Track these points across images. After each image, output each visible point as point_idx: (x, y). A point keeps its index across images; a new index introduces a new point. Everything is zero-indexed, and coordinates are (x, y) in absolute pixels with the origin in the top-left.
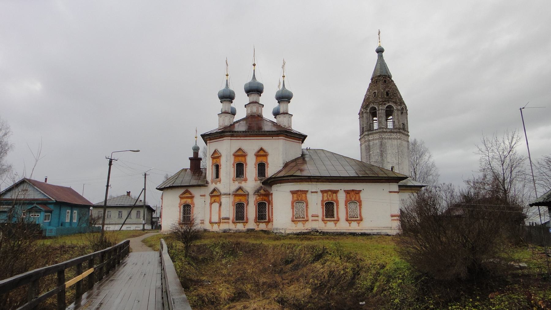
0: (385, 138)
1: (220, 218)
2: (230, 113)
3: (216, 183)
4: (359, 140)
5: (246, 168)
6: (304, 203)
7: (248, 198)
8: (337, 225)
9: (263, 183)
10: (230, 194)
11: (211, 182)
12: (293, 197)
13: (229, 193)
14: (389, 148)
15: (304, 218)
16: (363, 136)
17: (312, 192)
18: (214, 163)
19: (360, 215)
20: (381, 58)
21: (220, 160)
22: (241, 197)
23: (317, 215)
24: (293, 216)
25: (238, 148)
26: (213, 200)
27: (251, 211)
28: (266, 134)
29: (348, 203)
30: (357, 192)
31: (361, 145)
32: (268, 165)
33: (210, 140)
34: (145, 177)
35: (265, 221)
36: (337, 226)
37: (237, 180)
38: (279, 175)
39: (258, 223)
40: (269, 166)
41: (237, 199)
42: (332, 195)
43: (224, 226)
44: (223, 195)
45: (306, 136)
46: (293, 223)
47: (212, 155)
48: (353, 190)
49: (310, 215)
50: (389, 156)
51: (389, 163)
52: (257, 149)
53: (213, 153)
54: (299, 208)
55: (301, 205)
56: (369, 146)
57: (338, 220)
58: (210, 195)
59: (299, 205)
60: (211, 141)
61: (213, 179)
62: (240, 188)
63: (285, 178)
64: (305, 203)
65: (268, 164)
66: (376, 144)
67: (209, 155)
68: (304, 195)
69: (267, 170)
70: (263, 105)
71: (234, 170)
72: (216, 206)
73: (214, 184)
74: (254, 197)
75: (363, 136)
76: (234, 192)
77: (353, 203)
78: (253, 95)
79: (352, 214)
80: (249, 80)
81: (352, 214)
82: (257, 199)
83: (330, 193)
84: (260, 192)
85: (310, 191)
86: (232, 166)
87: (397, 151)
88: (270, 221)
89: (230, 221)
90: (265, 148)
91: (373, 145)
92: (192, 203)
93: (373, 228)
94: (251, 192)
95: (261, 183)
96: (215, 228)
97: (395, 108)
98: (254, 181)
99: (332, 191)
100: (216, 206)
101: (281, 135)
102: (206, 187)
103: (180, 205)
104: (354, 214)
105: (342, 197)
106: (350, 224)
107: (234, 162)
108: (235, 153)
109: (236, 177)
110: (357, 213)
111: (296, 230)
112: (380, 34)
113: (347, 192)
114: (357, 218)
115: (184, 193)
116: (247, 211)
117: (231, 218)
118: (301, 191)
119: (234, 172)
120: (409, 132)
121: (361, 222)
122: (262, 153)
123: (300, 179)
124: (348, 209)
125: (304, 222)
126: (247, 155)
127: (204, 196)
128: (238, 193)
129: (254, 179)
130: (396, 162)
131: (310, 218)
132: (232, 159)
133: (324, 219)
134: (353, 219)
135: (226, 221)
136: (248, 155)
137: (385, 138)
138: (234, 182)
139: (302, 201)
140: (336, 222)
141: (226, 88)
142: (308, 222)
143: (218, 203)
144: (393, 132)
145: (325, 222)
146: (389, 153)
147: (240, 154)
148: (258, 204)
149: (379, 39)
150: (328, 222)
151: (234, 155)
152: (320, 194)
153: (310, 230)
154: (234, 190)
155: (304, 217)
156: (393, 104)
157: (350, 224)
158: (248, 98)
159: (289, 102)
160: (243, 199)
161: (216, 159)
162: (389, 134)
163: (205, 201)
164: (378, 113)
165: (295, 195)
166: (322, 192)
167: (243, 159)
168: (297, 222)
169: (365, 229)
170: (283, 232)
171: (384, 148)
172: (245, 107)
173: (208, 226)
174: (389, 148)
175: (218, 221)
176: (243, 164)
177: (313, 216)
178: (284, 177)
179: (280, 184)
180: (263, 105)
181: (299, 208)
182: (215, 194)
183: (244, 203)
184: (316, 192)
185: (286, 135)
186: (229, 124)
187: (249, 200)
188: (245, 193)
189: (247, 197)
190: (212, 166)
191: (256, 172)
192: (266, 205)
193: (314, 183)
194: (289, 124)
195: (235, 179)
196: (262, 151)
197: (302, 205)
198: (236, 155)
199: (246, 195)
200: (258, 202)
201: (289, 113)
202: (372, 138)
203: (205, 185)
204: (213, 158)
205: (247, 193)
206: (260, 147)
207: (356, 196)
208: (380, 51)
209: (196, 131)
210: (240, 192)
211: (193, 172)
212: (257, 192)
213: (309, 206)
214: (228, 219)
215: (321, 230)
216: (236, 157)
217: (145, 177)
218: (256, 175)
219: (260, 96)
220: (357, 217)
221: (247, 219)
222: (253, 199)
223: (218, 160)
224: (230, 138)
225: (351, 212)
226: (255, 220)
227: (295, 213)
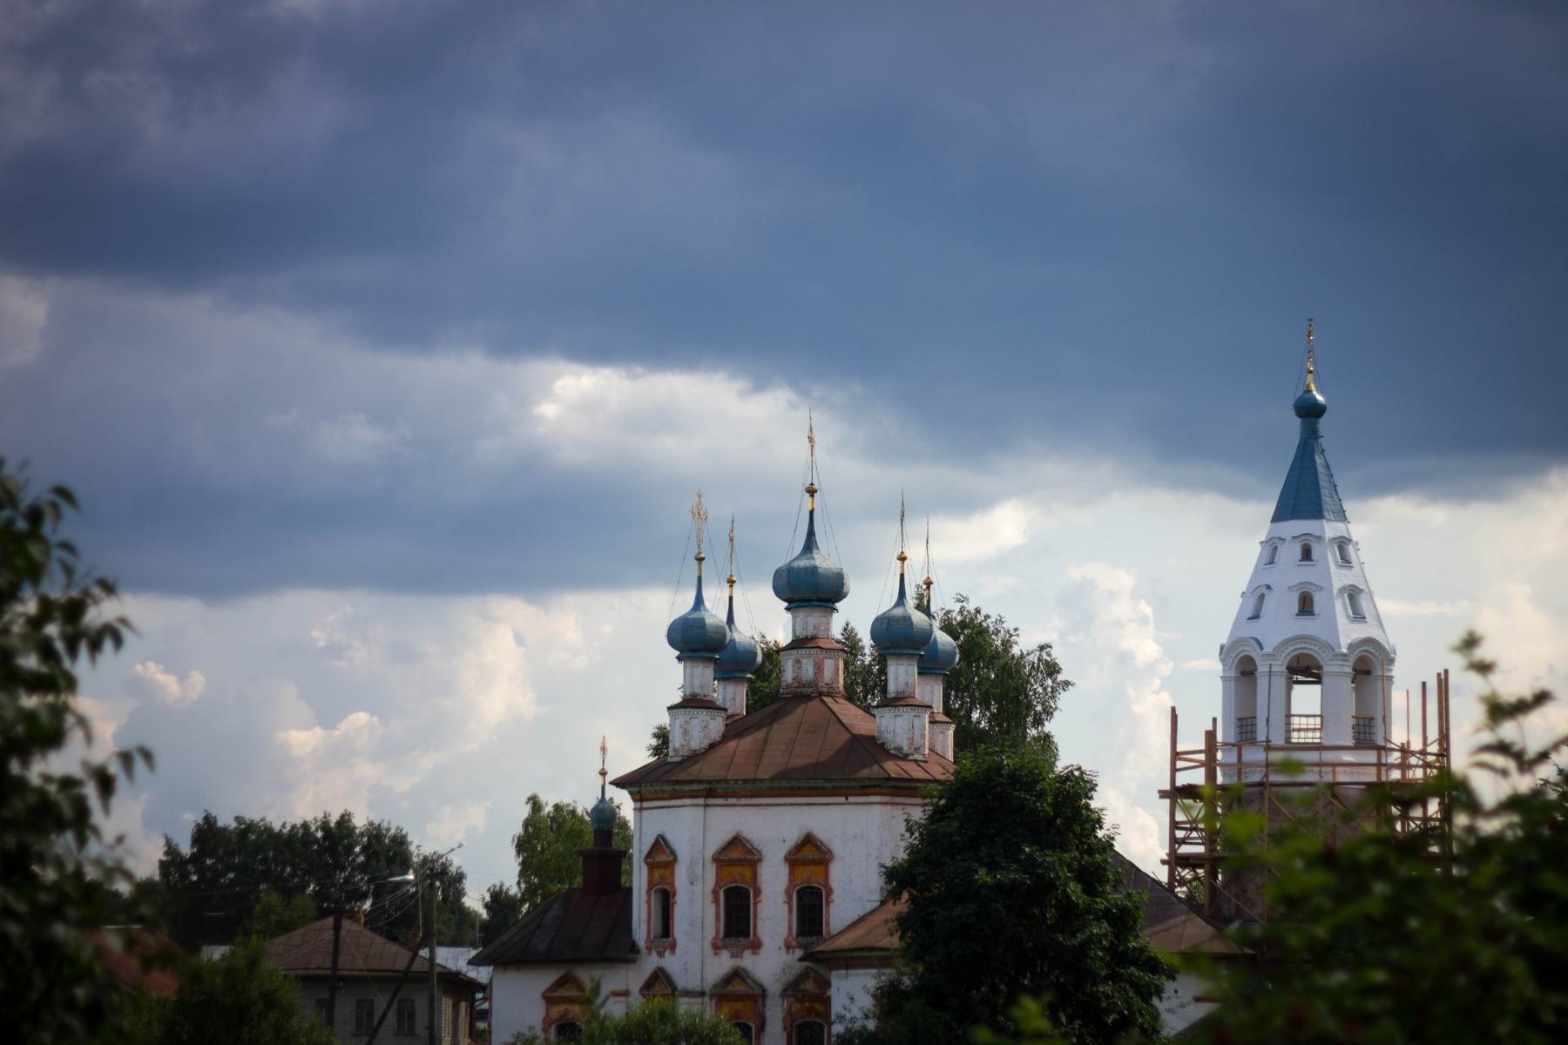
3: (661, 954)
5: (755, 904)
7: (764, 1005)
10: (702, 994)
13: (699, 989)
21: (672, 874)
25: (727, 837)
28: (823, 788)
32: (830, 895)
37: (725, 947)
40: (834, 897)
47: (649, 855)
52: (793, 837)
60: (645, 804)
62: (737, 975)
65: (830, 891)
67: (640, 851)
69: (828, 913)
71: (717, 913)
73: (654, 953)
74: (783, 1005)
76: (715, 986)
78: (802, 614)
80: (787, 550)
82: (794, 1009)
84: (802, 986)
86: (710, 897)
90: (822, 834)
94: (773, 986)
98: (784, 951)
101: (873, 790)
102: (631, 965)
107: (717, 884)
115: (559, 984)
119: (717, 919)
122: (808, 853)
126: (760, 860)
128: (730, 988)
129: (783, 946)
154: (718, 980)
161: (662, 871)
167: (747, 873)
176: (748, 892)
187: (768, 1013)
190: (649, 892)
191: (790, 920)
195: (720, 944)
196: (809, 845)
200: (798, 1022)
203: (627, 953)
206: (804, 831)
209: (603, 749)
210: (738, 987)
212: (793, 989)
218: (790, 928)
223: (667, 873)
224: (701, 801)
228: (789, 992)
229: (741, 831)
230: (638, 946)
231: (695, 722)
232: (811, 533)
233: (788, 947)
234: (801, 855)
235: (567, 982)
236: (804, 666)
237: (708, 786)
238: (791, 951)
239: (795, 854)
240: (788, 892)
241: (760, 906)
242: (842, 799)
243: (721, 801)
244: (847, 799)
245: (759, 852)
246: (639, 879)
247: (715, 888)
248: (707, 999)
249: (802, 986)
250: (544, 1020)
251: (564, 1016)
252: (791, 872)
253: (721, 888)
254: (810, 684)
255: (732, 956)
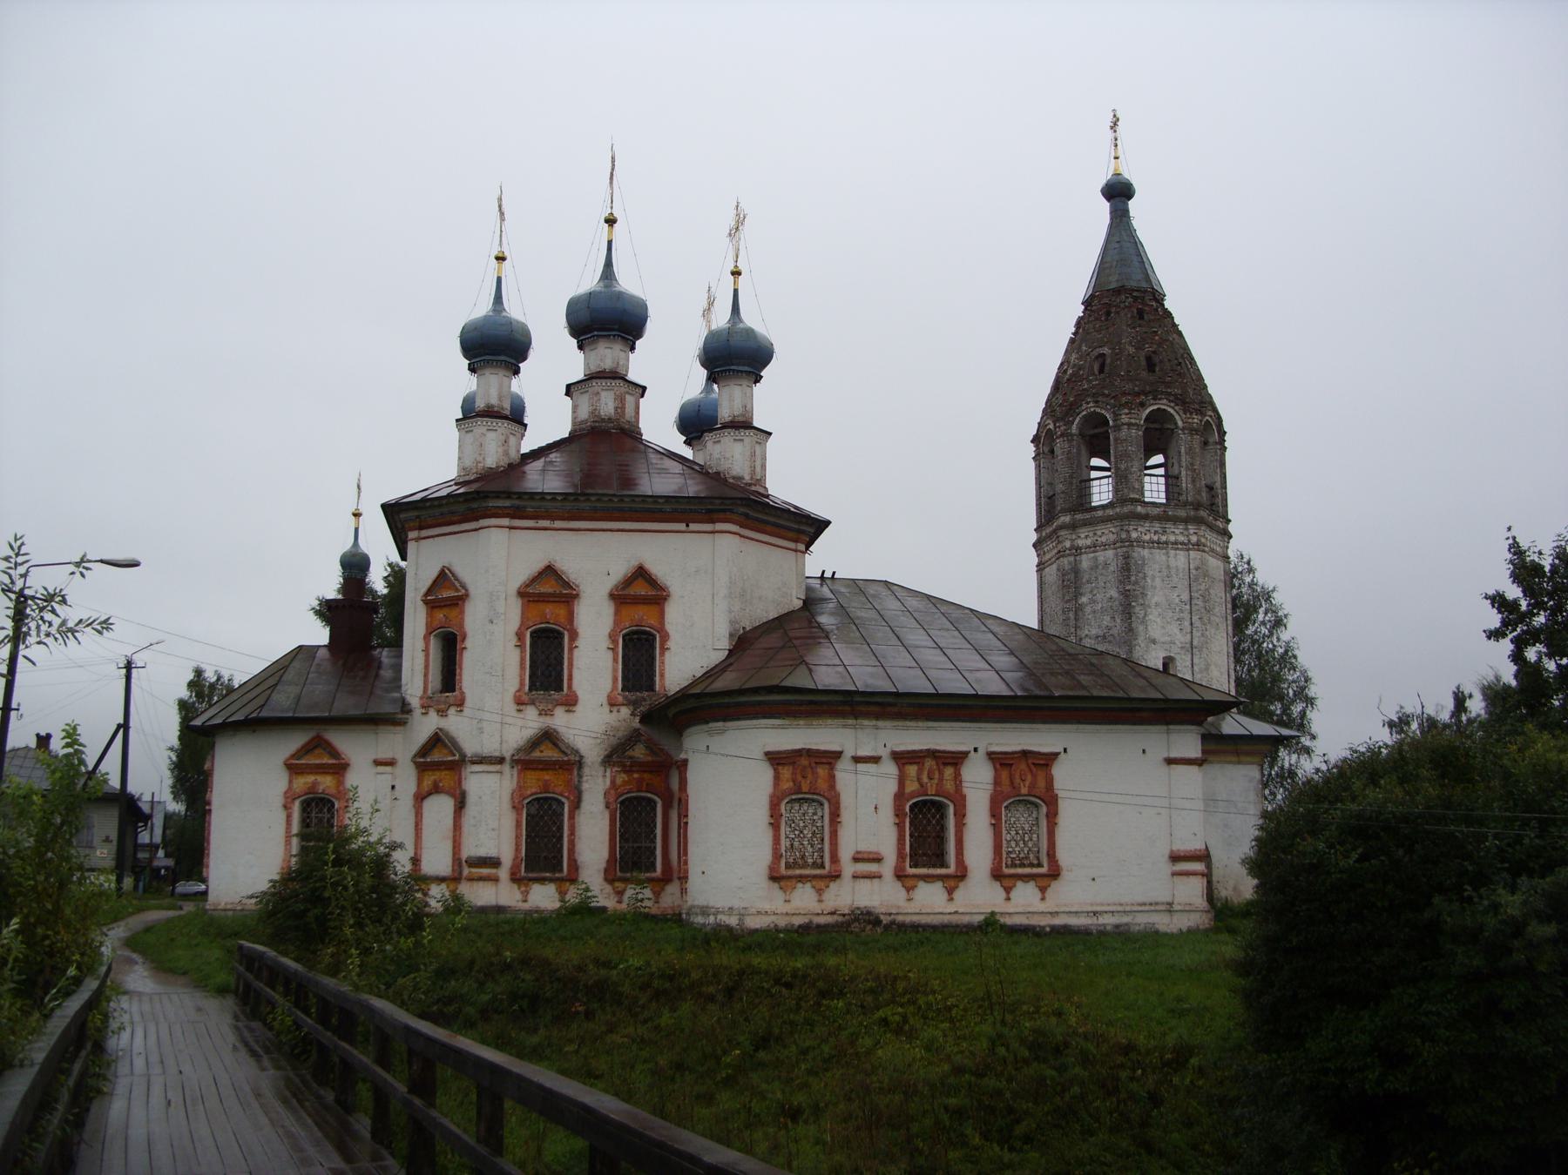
0: (1141, 543)
1: (460, 859)
2: (505, 418)
3: (442, 713)
4: (1035, 545)
5: (571, 650)
6: (822, 804)
7: (580, 776)
8: (958, 894)
9: (646, 719)
10: (501, 760)
11: (423, 707)
12: (777, 778)
13: (497, 754)
14: (1158, 582)
15: (822, 866)
16: (1049, 530)
17: (857, 760)
18: (436, 623)
19: (1048, 855)
21: (462, 612)
22: (550, 772)
23: (875, 856)
24: (777, 855)
25: (538, 566)
26: (428, 782)
28: (661, 511)
29: (1005, 804)
30: (1042, 762)
31: (1041, 567)
33: (421, 528)
34: (128, 678)
35: (648, 875)
36: (955, 902)
37: (533, 703)
38: (720, 684)
39: (619, 885)
40: (670, 644)
41: (534, 782)
42: (941, 773)
44: (474, 763)
45: (827, 523)
46: (776, 885)
47: (429, 592)
48: (1025, 754)
49: (846, 854)
50: (1153, 615)
51: (1154, 642)
52: (619, 569)
53: (435, 582)
54: (802, 824)
55: (811, 811)
56: (1076, 571)
57: (962, 875)
58: (415, 763)
59: (802, 811)
60: (425, 533)
61: (429, 692)
62: (548, 737)
63: (743, 699)
64: (826, 806)
65: (665, 637)
66: (1106, 564)
68: (822, 771)
69: (663, 663)
70: (644, 389)
71: (522, 660)
73: (433, 714)
74: (604, 776)
75: (1049, 530)
76: (519, 750)
77: (1021, 808)
79: (1017, 849)
81: (1017, 849)
82: (619, 781)
83: (929, 763)
84: (630, 753)
85: (849, 752)
86: (514, 641)
87: (1185, 597)
88: (675, 874)
89: (504, 873)
90: (657, 569)
91: (1095, 567)
92: (339, 792)
93: (1098, 909)
95: (633, 714)
97: (1180, 423)
98: (606, 708)
99: (940, 757)
100: (439, 809)
101: (721, 515)
102: (398, 728)
103: (289, 797)
104: (1026, 850)
105: (978, 780)
106: (1008, 890)
107: (522, 623)
108: (527, 586)
109: (530, 690)
110: (1037, 845)
111: (787, 914)
112: (1119, 128)
113: (1000, 761)
114: (1040, 865)
115: (306, 750)
116: (572, 833)
117: (507, 858)
118: (809, 753)
120: (1230, 521)
121: (1055, 885)
123: (811, 703)
124: (1004, 832)
125: (821, 884)
126: (577, 596)
127: (391, 763)
129: (605, 702)
130: (1182, 639)
131: (848, 868)
132: (512, 614)
133: (903, 869)
134: (1020, 871)
135: (485, 871)
136: (582, 594)
137: (1141, 543)
138: (521, 707)
139: (815, 797)
140: (952, 883)
141: (494, 310)
142: (838, 881)
143: (453, 795)
144: (1176, 520)
145: (910, 883)
146: (1157, 605)
148: (622, 803)
149: (1116, 146)
150: (921, 884)
151: (522, 594)
152: (890, 768)
153: (844, 915)
154: (521, 743)
155: (819, 861)
156: (1172, 404)
157: (1008, 890)
158: (580, 356)
159: (758, 379)
160: (556, 781)
161: (445, 611)
162: (1157, 526)
163: (393, 787)
164: (1116, 440)
165: (786, 772)
166: (902, 759)
167: (561, 611)
168: (794, 881)
169: (1067, 910)
170: (733, 921)
171: (1136, 583)
172: (568, 394)
174: (1158, 582)
175: (450, 869)
177: (860, 856)
178: (741, 692)
179: (720, 724)
180: (644, 389)
181: (802, 824)
182: (436, 756)
183: (563, 800)
184: (875, 760)
185: (747, 516)
186: (504, 462)
187: (585, 786)
188: (566, 759)
189: (575, 773)
190: (426, 638)
191: (615, 670)
192: (654, 809)
193: (866, 722)
194: (753, 472)
195: (525, 698)
197: (815, 814)
198: (528, 595)
199: (570, 764)
201: (756, 424)
202: (1088, 542)
203: (397, 717)
204: (433, 602)
205: (577, 759)
206: (635, 563)
207: (1034, 776)
208: (1118, 193)
209: (359, 487)
210: (548, 753)
211: (341, 662)
212: (616, 755)
213: (846, 816)
214: (494, 863)
215: (890, 914)
216: (531, 605)
217: (128, 678)
218: (615, 680)
219: (632, 348)
220: (1035, 862)
221: (575, 866)
222: (601, 779)
223: (453, 613)
224: (506, 521)
225: (1013, 844)
226: (606, 871)
227: (784, 843)
228: (615, 758)
229: (555, 561)
230: (409, 704)
231: (491, 435)
232: (609, 264)
233: (612, 704)
234: (631, 591)
235: (315, 747)
236: (603, 400)
237: (517, 502)
238: (615, 709)
239: (623, 589)
240: (612, 637)
241: (576, 653)
242: (682, 526)
243: (531, 523)
244: (687, 526)
245: (578, 586)
246: (415, 621)
247: (519, 629)
248: (506, 768)
249: (630, 753)
250: (286, 793)
251: (312, 788)
252: (617, 612)
253: (527, 629)
254: (609, 419)
255: (540, 714)
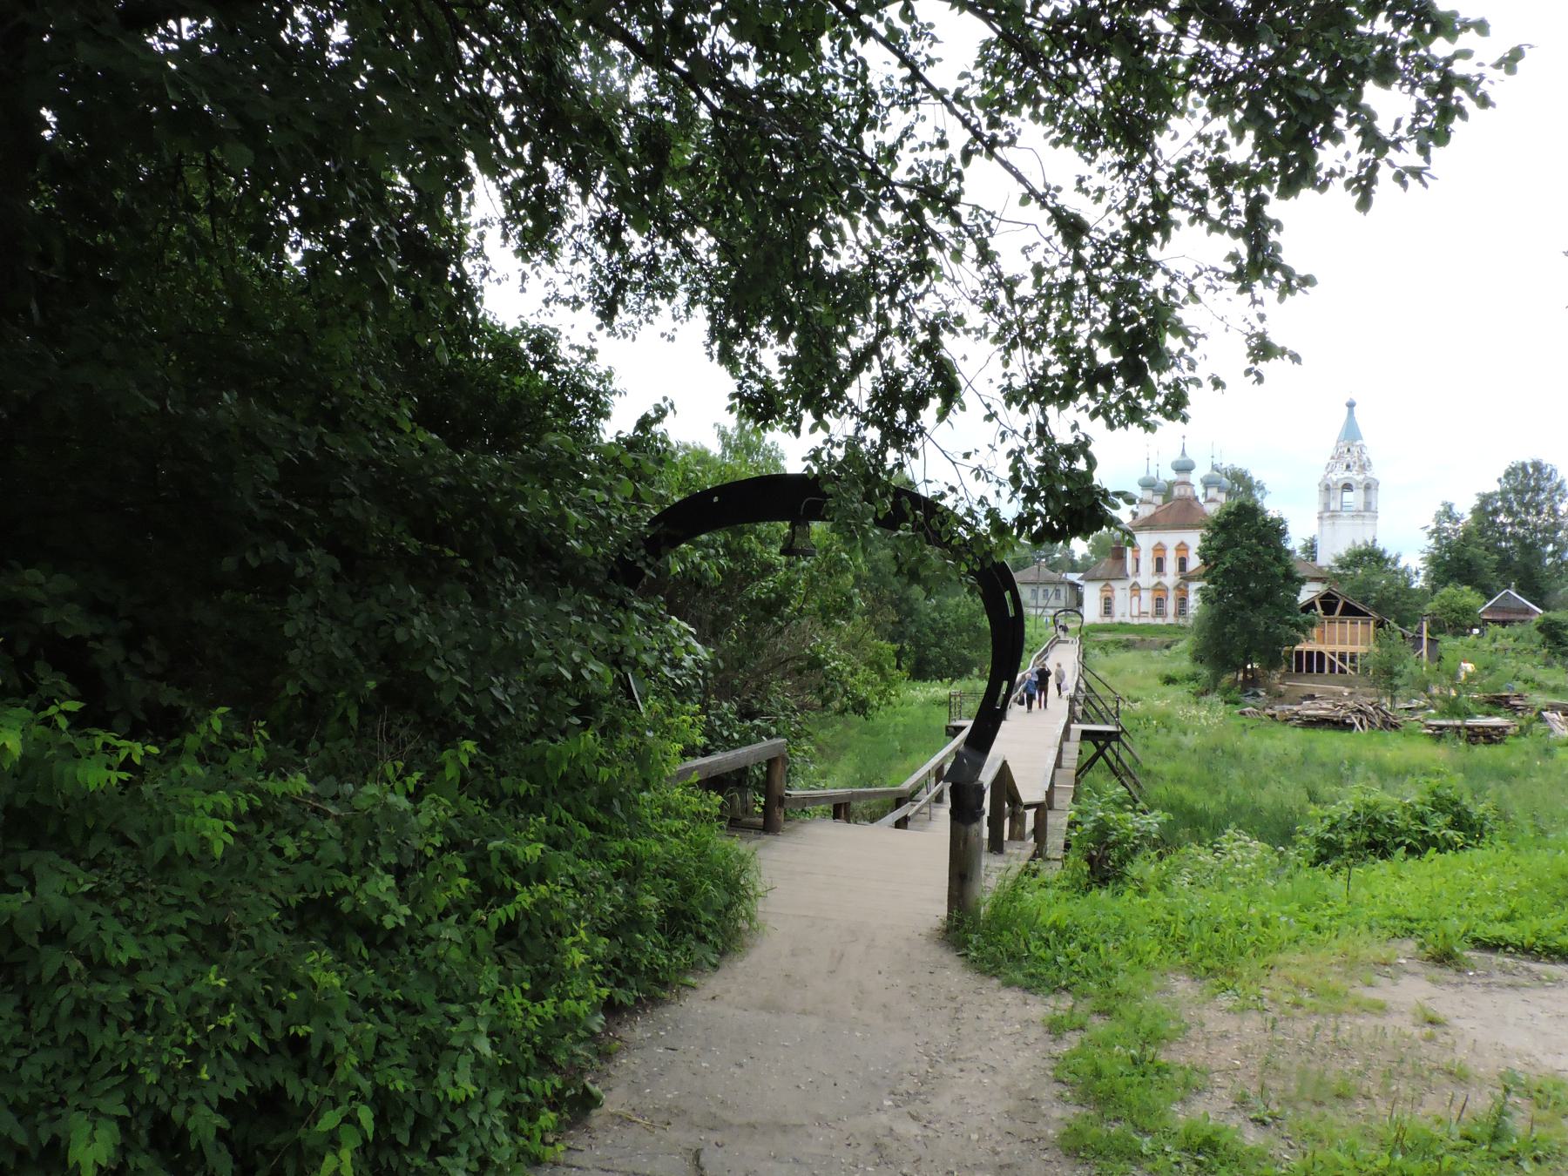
20: (1351, 413)
27: (1171, 606)
43: (1143, 621)
52: (1177, 542)
72: (1136, 599)
80: (1177, 456)
96: (1136, 621)
100: (1136, 599)
147: (1160, 549)
173: (1128, 619)
199: (1166, 590)
208: (1351, 405)
212: (1177, 588)
